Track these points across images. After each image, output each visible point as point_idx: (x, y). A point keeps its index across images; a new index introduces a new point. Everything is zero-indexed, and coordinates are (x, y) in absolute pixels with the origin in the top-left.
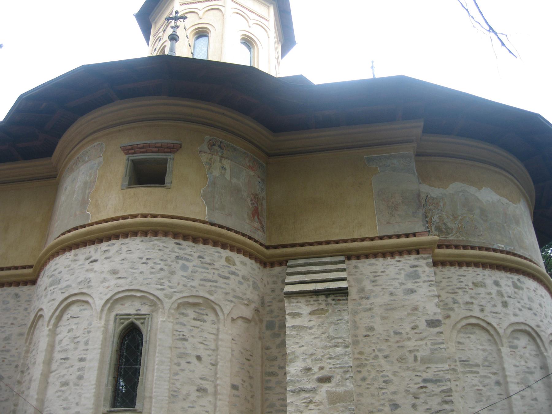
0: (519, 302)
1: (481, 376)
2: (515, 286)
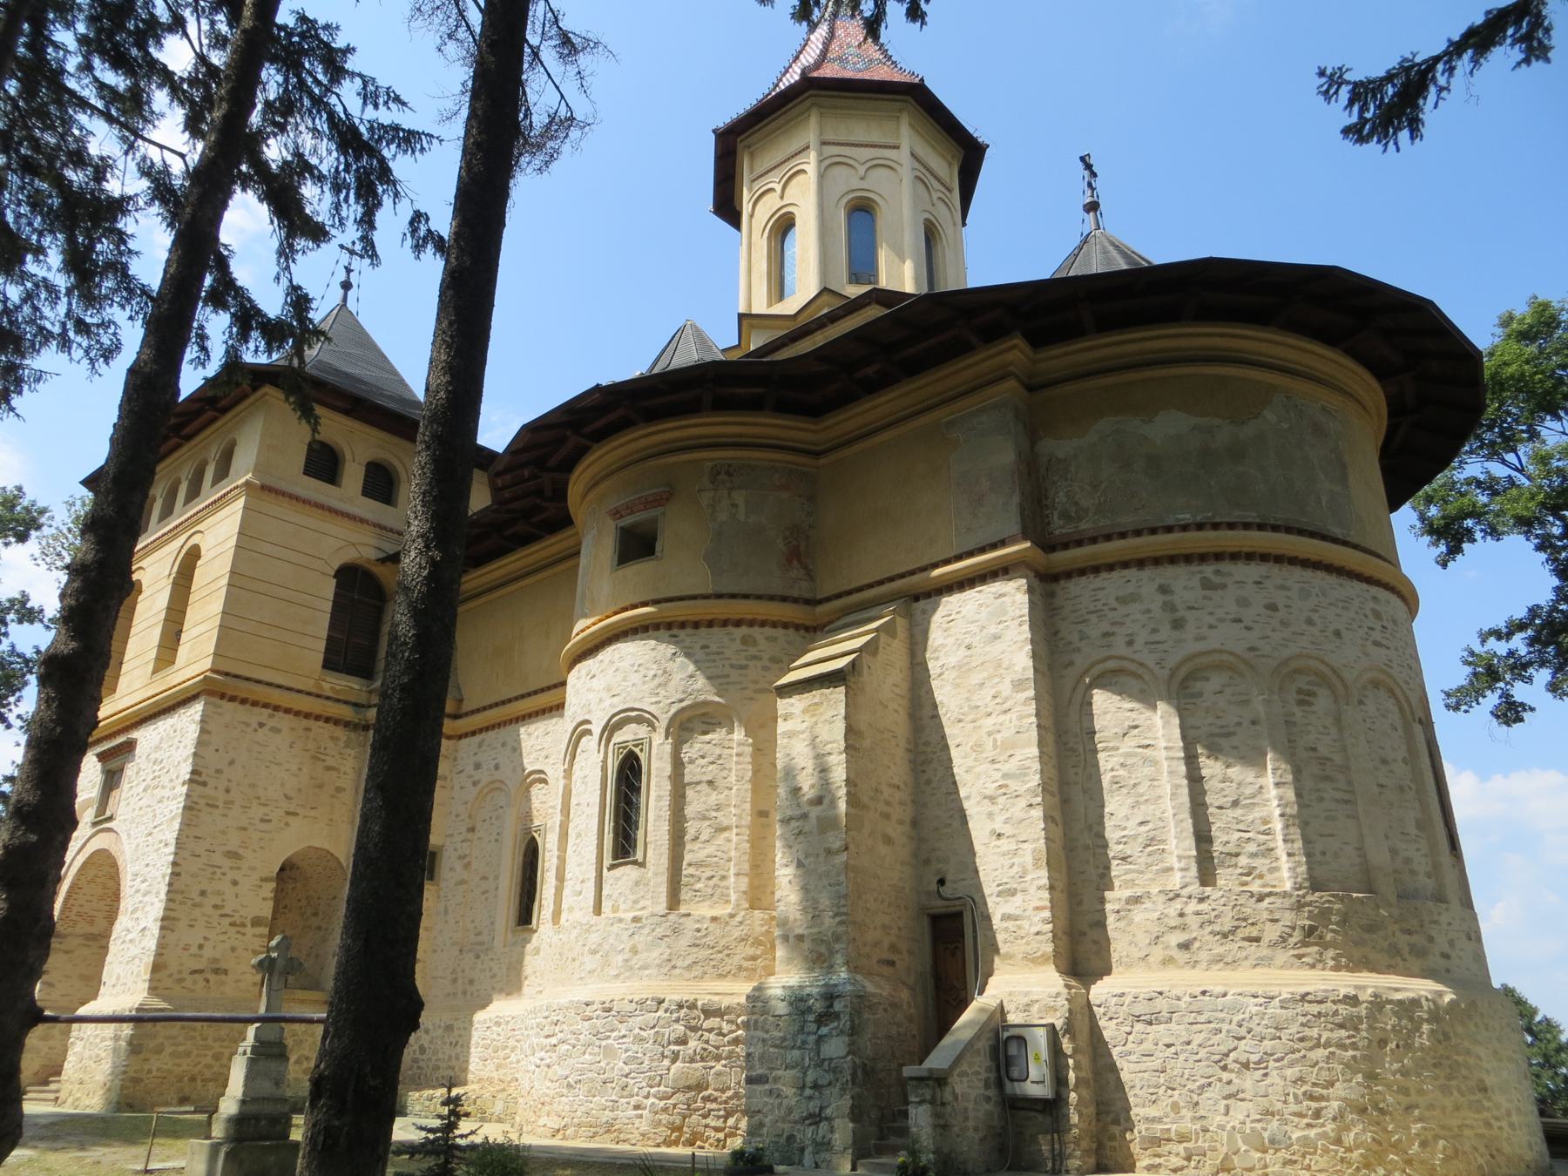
0: (1211, 614)
1: (1122, 755)
2: (1207, 585)
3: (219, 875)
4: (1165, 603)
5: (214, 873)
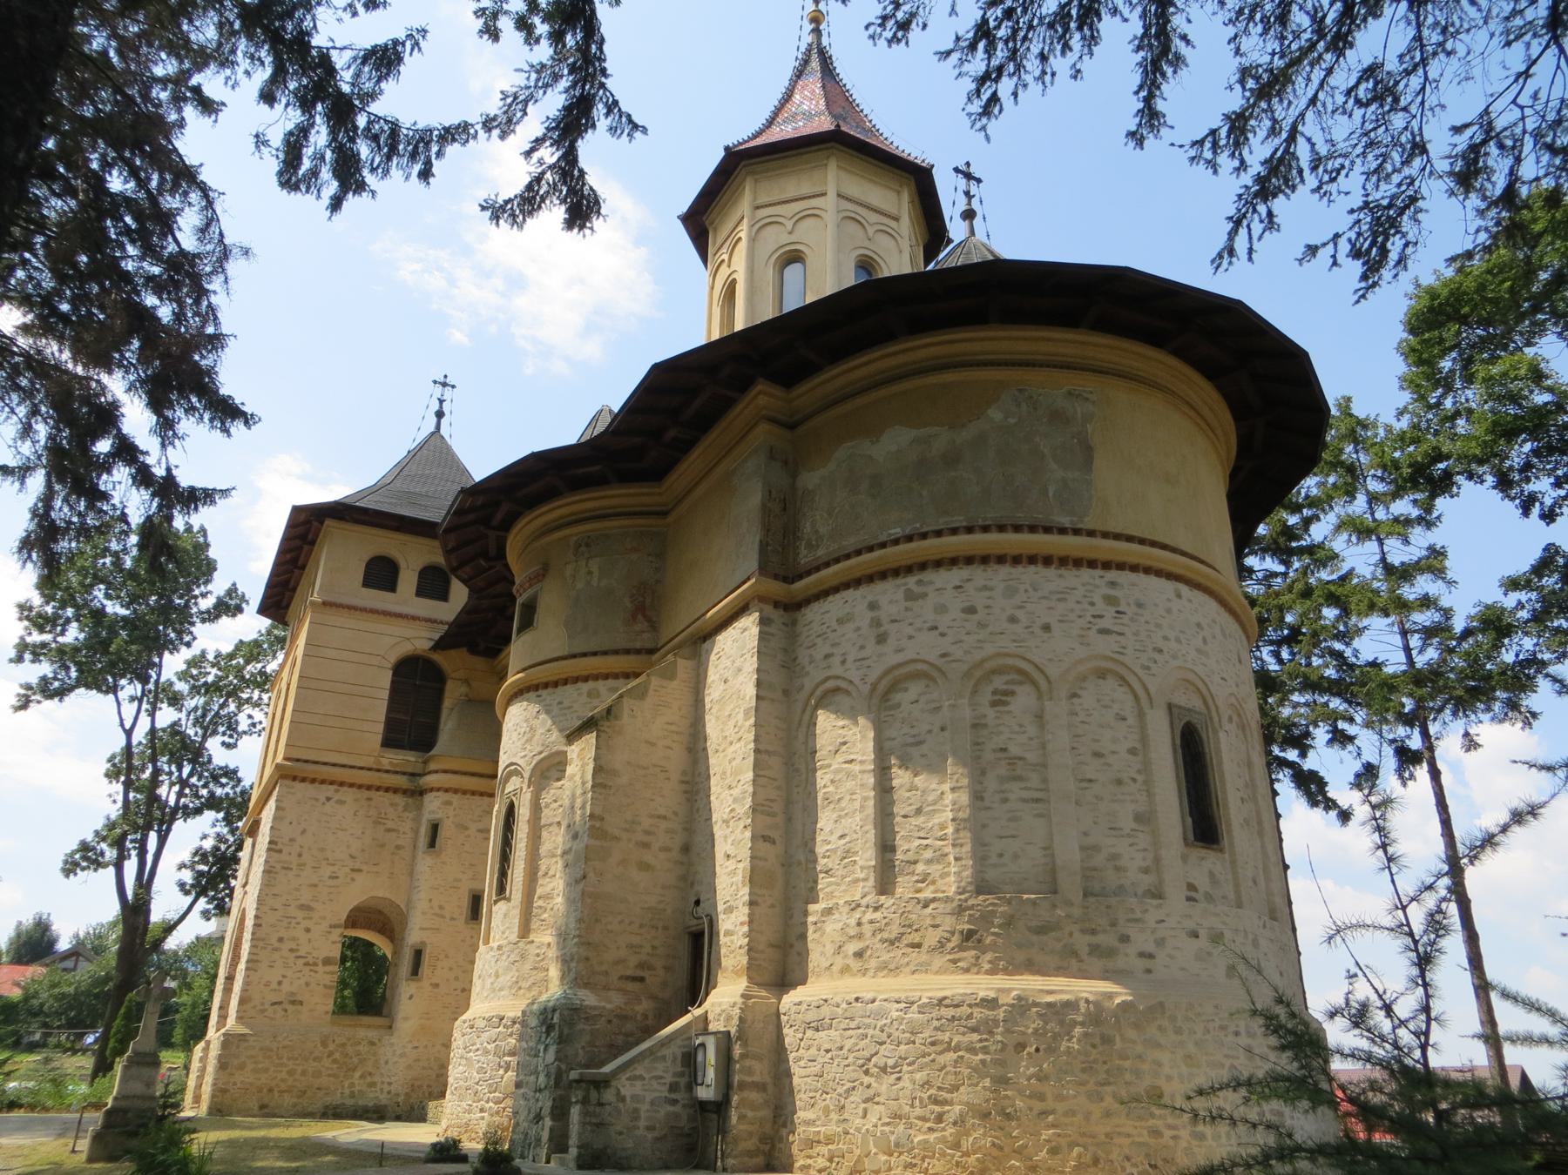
2: (910, 596)
3: (293, 925)
4: (872, 619)
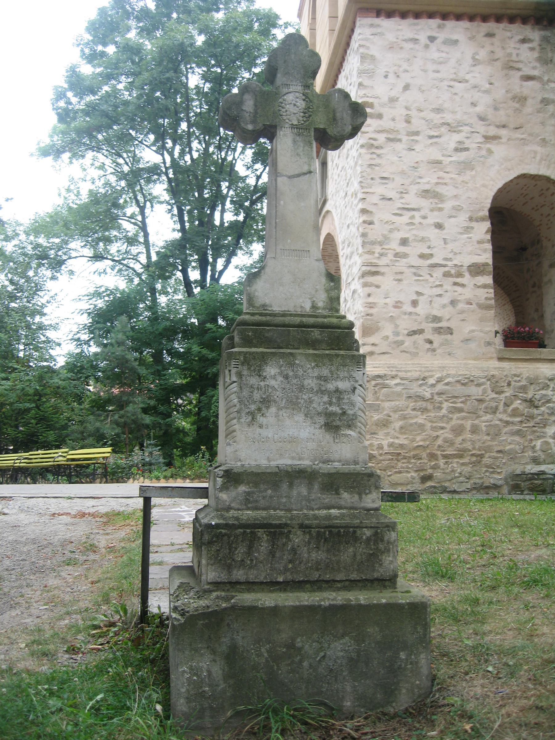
3: (417, 220)
5: (413, 217)
